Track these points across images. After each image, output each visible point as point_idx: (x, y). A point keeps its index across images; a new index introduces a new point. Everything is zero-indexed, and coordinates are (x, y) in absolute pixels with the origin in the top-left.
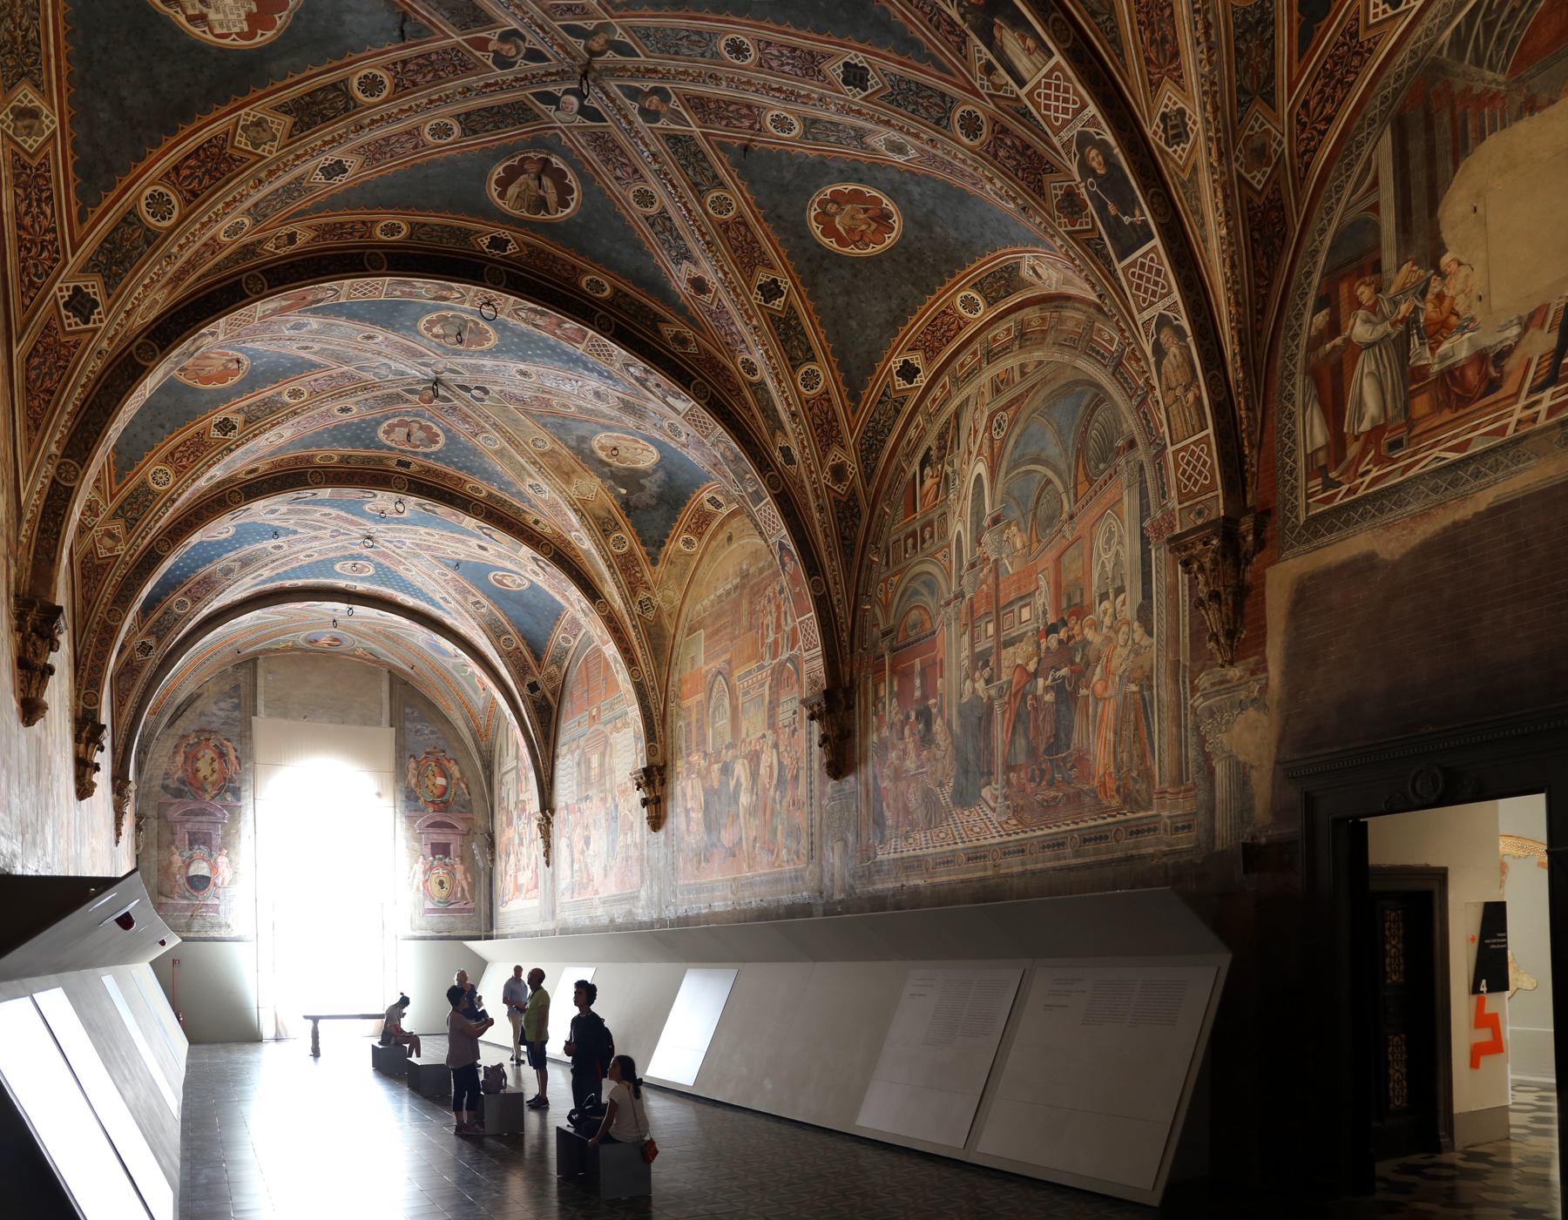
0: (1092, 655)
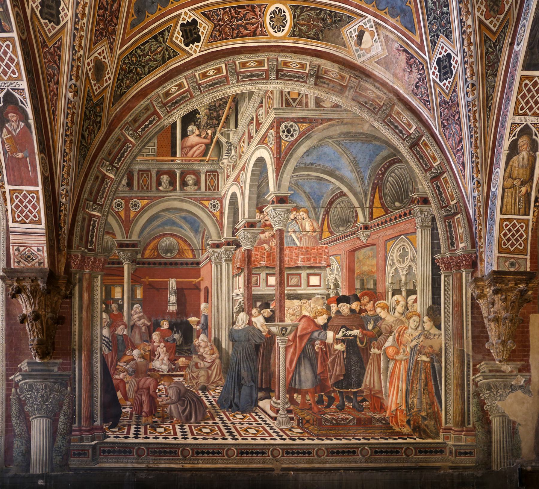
0: (384, 328)
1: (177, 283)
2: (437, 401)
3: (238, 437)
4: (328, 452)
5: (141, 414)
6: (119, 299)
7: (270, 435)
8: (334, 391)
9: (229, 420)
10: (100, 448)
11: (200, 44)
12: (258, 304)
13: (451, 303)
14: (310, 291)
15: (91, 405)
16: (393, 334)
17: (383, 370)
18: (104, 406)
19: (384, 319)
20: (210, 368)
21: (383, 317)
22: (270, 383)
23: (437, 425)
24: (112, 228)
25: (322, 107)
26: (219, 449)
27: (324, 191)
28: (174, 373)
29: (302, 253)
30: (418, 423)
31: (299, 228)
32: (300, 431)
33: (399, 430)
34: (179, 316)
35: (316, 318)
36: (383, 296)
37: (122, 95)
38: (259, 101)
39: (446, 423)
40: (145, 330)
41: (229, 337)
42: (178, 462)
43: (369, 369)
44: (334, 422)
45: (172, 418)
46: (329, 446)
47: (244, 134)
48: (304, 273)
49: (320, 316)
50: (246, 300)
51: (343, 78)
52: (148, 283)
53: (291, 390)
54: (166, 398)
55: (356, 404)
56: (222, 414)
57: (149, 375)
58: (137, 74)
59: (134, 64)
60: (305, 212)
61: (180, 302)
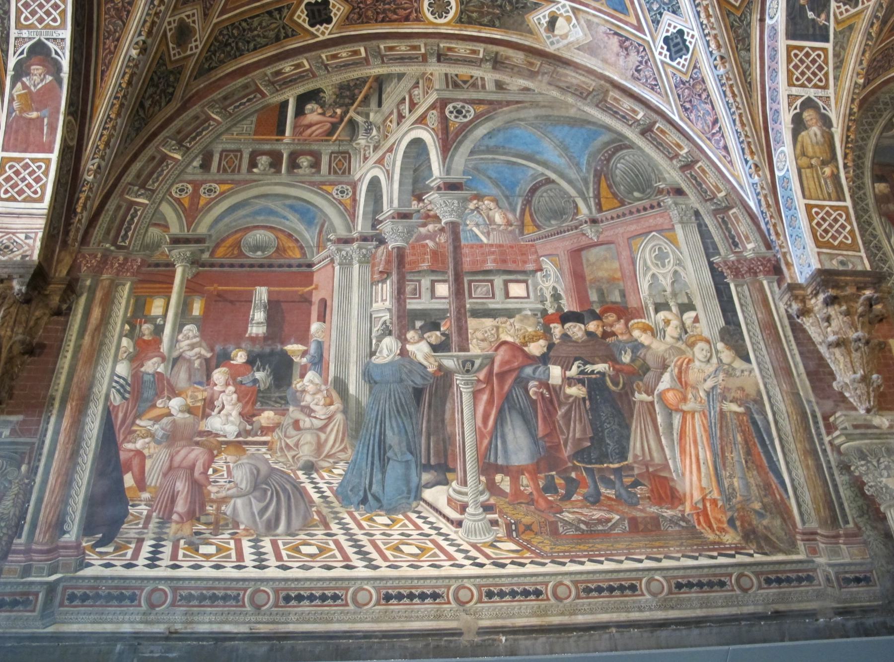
0: (651, 361)
1: (270, 293)
2: (776, 481)
3: (379, 561)
4: (577, 588)
5: (170, 517)
6: (157, 317)
7: (450, 558)
8: (575, 468)
9: (361, 527)
10: (65, 589)
11: (330, 26)
12: (418, 324)
13: (756, 323)
14: (511, 305)
15: (65, 499)
16: (669, 369)
17: (664, 429)
18: (92, 502)
19: (648, 348)
20: (322, 429)
21: (646, 343)
22: (446, 456)
23: (787, 525)
24: (165, 219)
25: (505, 89)
26: (337, 588)
27: (520, 176)
28: (250, 439)
29: (493, 253)
30: (750, 524)
31: (484, 220)
32: (514, 547)
33: (717, 539)
34: (270, 342)
35: (526, 346)
36: (639, 312)
37: (211, 69)
38: (414, 81)
39: (804, 523)
40: (201, 364)
41: (364, 374)
42: (242, 618)
43: (636, 427)
44: (583, 526)
45: (236, 525)
46: (578, 578)
47: (391, 113)
48: (498, 281)
49: (533, 342)
50: (395, 318)
51: (531, 64)
52: (215, 293)
53: (488, 468)
54: (228, 486)
55: (622, 491)
56: (346, 516)
57: (197, 443)
58: (238, 48)
59: (235, 38)
60: (492, 201)
61: (271, 321)
